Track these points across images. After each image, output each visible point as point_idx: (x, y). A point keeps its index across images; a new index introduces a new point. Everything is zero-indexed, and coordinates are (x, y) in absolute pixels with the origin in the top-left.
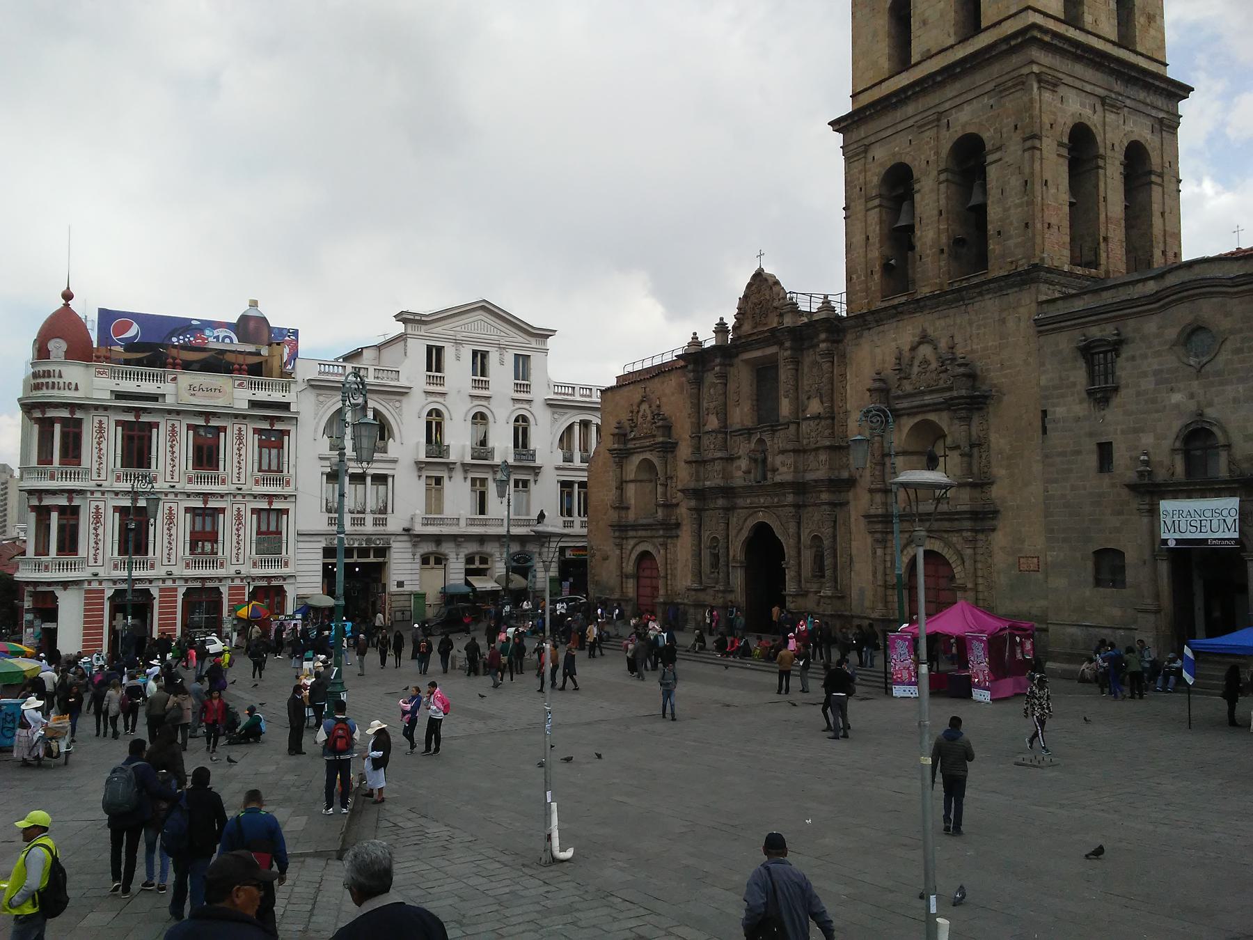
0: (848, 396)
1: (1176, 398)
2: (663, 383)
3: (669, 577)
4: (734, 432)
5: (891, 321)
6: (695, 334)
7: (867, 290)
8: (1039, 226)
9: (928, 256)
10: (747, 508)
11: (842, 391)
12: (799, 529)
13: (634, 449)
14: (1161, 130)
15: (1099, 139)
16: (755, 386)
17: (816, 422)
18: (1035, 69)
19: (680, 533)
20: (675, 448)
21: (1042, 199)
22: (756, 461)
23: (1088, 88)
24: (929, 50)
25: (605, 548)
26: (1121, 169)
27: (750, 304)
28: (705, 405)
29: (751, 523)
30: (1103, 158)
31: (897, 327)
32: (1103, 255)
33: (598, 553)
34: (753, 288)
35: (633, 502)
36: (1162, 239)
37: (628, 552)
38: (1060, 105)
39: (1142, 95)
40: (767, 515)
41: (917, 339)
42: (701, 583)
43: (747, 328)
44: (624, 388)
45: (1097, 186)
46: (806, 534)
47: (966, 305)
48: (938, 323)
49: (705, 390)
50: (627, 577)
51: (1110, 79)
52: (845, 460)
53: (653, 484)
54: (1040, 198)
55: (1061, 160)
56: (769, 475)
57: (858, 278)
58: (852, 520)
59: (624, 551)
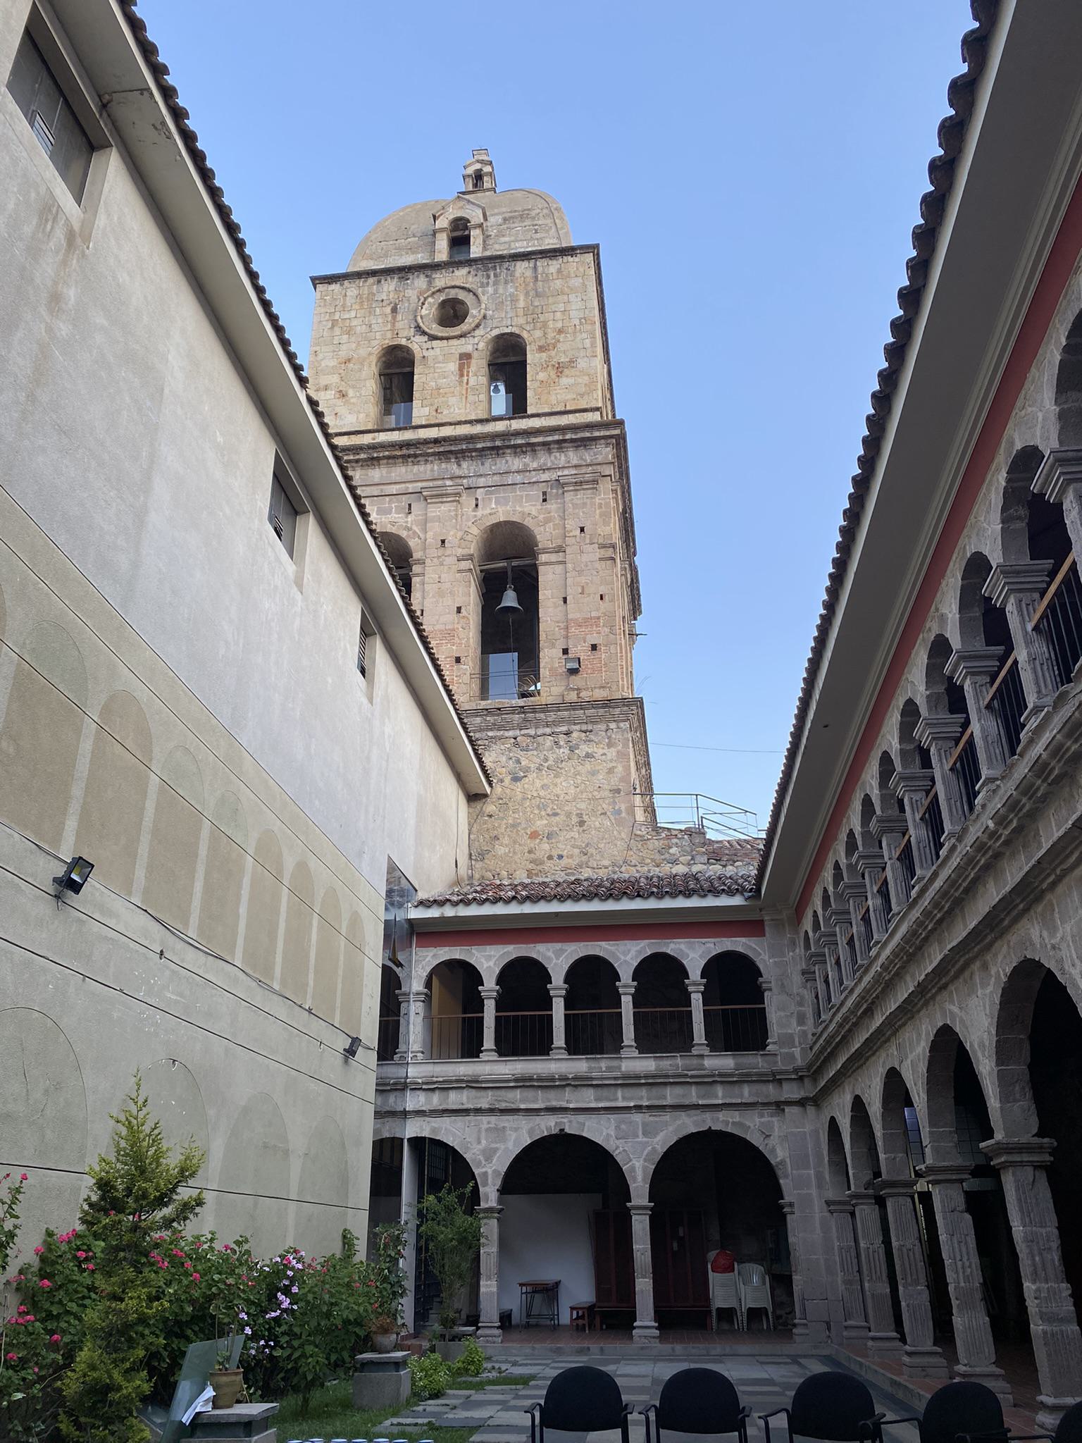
15: (412, 543)
23: (394, 489)
30: (421, 562)
39: (516, 463)
51: (444, 465)
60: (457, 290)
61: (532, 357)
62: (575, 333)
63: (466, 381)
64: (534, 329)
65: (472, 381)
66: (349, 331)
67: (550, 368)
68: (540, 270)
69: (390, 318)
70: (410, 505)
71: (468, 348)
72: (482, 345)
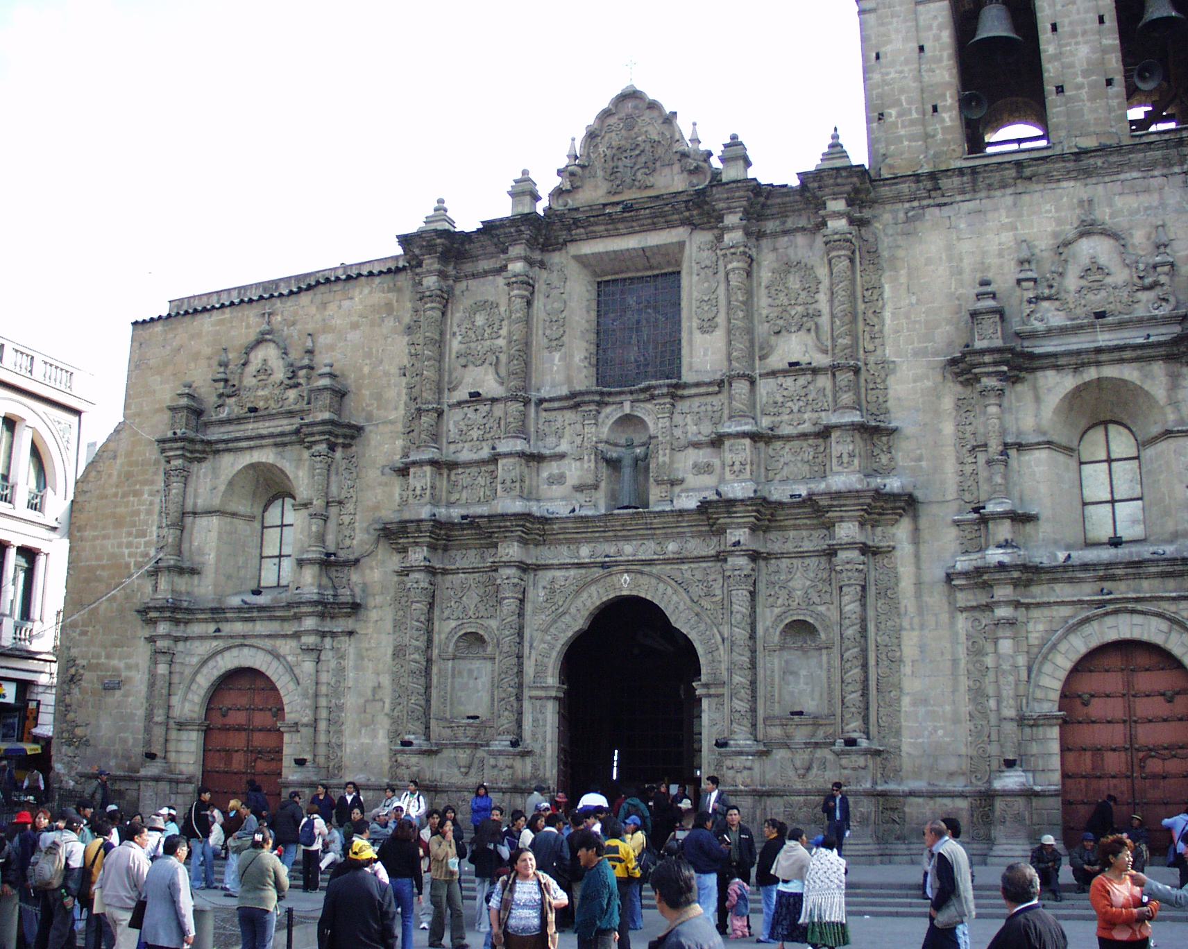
0: (887, 329)
2: (324, 305)
3: (322, 725)
4: (551, 400)
5: (998, 193)
6: (441, 201)
7: (927, 137)
9: (1079, 87)
10: (580, 566)
11: (875, 320)
12: (753, 607)
13: (227, 441)
16: (593, 314)
17: (802, 380)
19: (358, 627)
20: (353, 437)
22: (614, 464)
25: (115, 662)
27: (601, 149)
28: (455, 345)
29: (595, 597)
31: (1015, 204)
33: (88, 675)
34: (612, 120)
35: (211, 558)
37: (188, 671)
40: (644, 580)
41: (1070, 231)
42: (428, 739)
43: (593, 193)
44: (199, 317)
46: (768, 623)
48: (1119, 202)
49: (458, 315)
50: (181, 726)
52: (884, 459)
53: (257, 525)
56: (655, 493)
57: (900, 115)
58: (906, 584)
59: (177, 668)
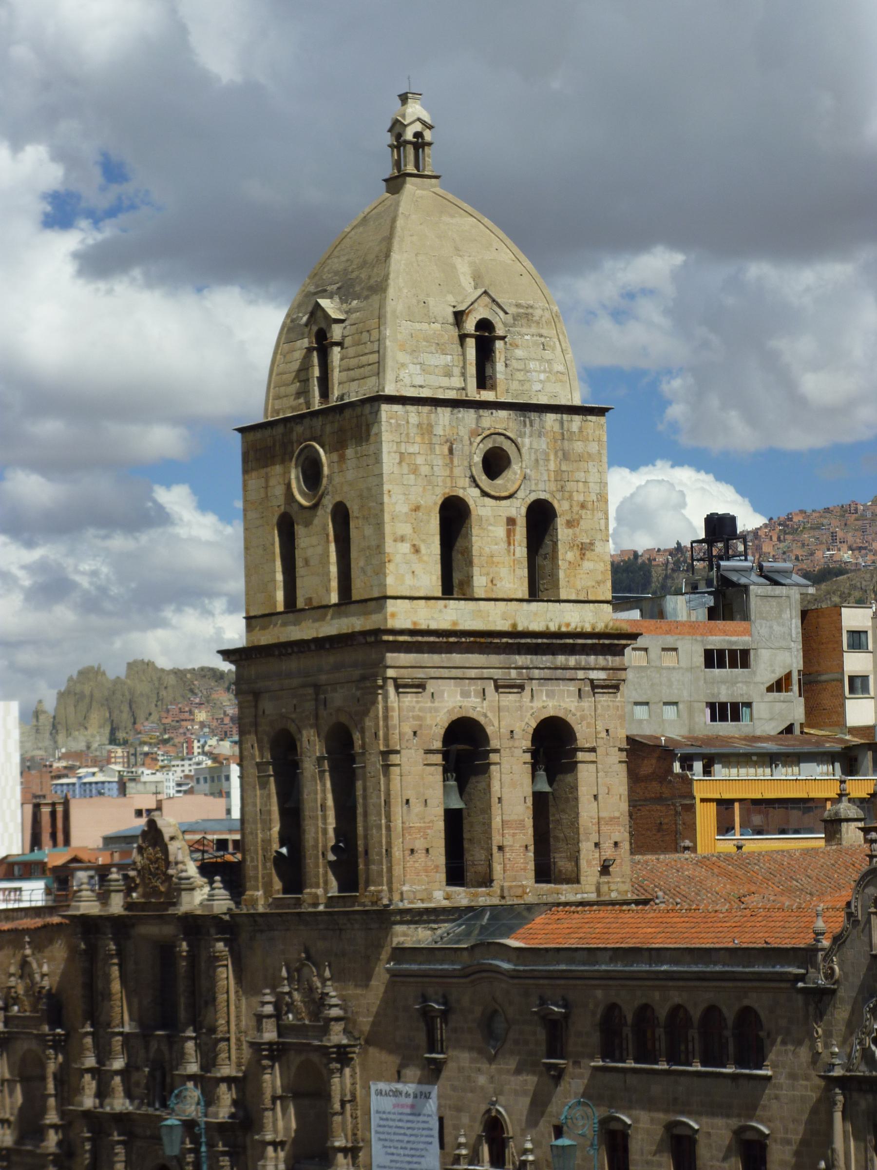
1: (482, 1080)
8: (397, 853)
14: (594, 694)
15: (489, 730)
18: (390, 673)
21: (403, 823)
23: (473, 673)
24: (310, 599)
26: (528, 757)
32: (497, 868)
36: (596, 828)
38: (429, 704)
39: (561, 659)
45: (489, 786)
47: (341, 930)
54: (400, 821)
55: (433, 768)
60: (502, 437)
61: (563, 533)
62: (593, 510)
63: (512, 551)
64: (563, 499)
65: (518, 554)
66: (415, 471)
67: (575, 548)
68: (566, 424)
69: (448, 458)
70: (484, 690)
71: (513, 513)
72: (523, 511)
